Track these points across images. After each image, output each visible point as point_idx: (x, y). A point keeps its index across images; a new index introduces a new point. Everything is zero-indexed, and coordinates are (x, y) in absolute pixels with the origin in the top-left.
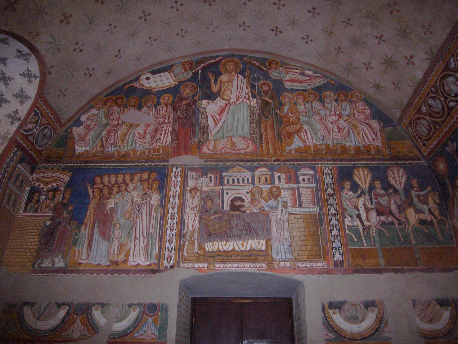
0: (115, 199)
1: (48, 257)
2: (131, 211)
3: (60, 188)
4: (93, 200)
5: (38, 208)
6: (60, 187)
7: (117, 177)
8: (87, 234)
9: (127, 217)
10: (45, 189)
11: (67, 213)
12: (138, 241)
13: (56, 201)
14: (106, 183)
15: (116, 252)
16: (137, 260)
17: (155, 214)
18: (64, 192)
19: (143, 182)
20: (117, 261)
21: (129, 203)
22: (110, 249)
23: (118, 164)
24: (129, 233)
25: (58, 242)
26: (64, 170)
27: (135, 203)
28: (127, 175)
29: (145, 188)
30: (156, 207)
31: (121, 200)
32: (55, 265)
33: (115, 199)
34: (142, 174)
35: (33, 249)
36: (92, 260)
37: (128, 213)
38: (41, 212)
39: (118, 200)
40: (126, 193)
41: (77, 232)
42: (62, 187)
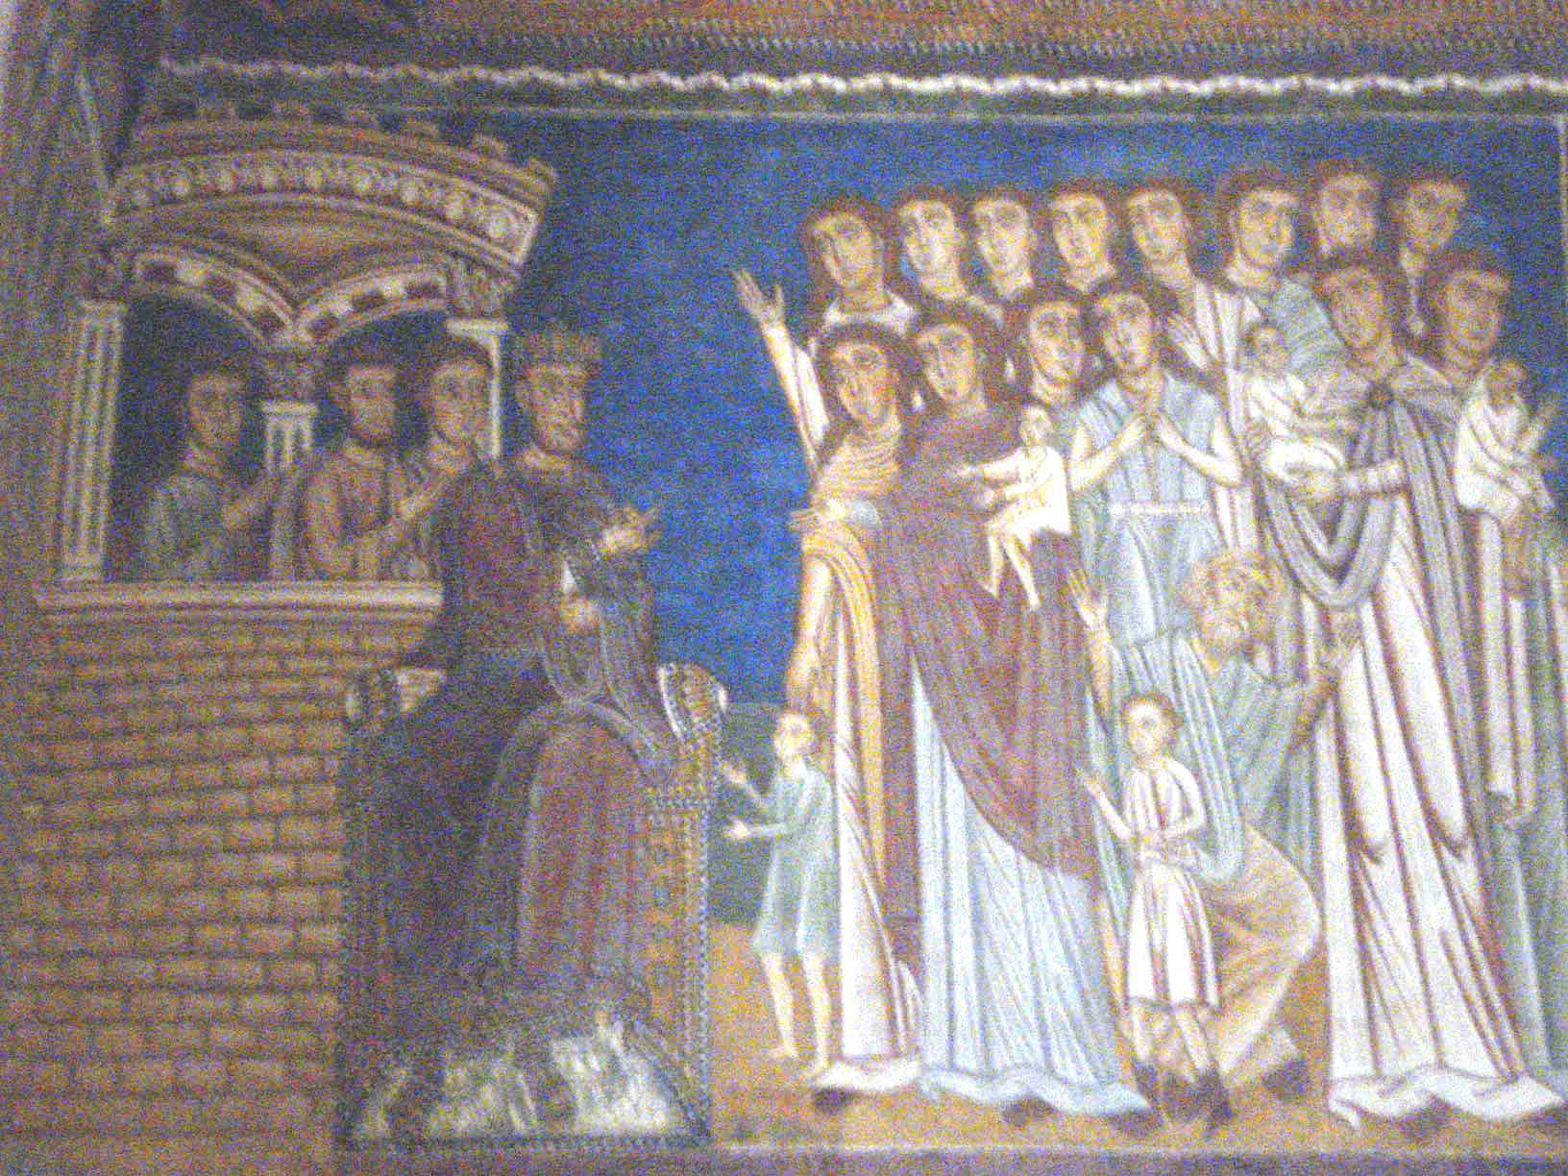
0: (1065, 452)
1: (481, 1043)
2: (1256, 575)
3: (457, 327)
4: (844, 454)
5: (261, 527)
6: (459, 314)
7: (1044, 225)
8: (845, 807)
9: (1228, 633)
10: (296, 334)
11: (589, 588)
12: (1384, 876)
13: (444, 458)
14: (946, 283)
15: (1182, 987)
16: (1411, 1061)
17: (1517, 607)
18: (514, 373)
19: (1335, 281)
20: (1211, 1081)
21: (1222, 495)
22: (1113, 954)
23: (1033, 83)
24: (1281, 794)
25: (562, 881)
26: (458, 128)
27: (1289, 493)
28: (1143, 200)
29: (1367, 334)
30: (1518, 533)
31: (1136, 466)
32: (567, 1112)
33: (1065, 452)
34: (1310, 197)
35: (298, 952)
36: (952, 1067)
37: (1227, 597)
38: (300, 575)
39: (1103, 462)
40: (1176, 388)
41: (739, 779)
42: (482, 315)
